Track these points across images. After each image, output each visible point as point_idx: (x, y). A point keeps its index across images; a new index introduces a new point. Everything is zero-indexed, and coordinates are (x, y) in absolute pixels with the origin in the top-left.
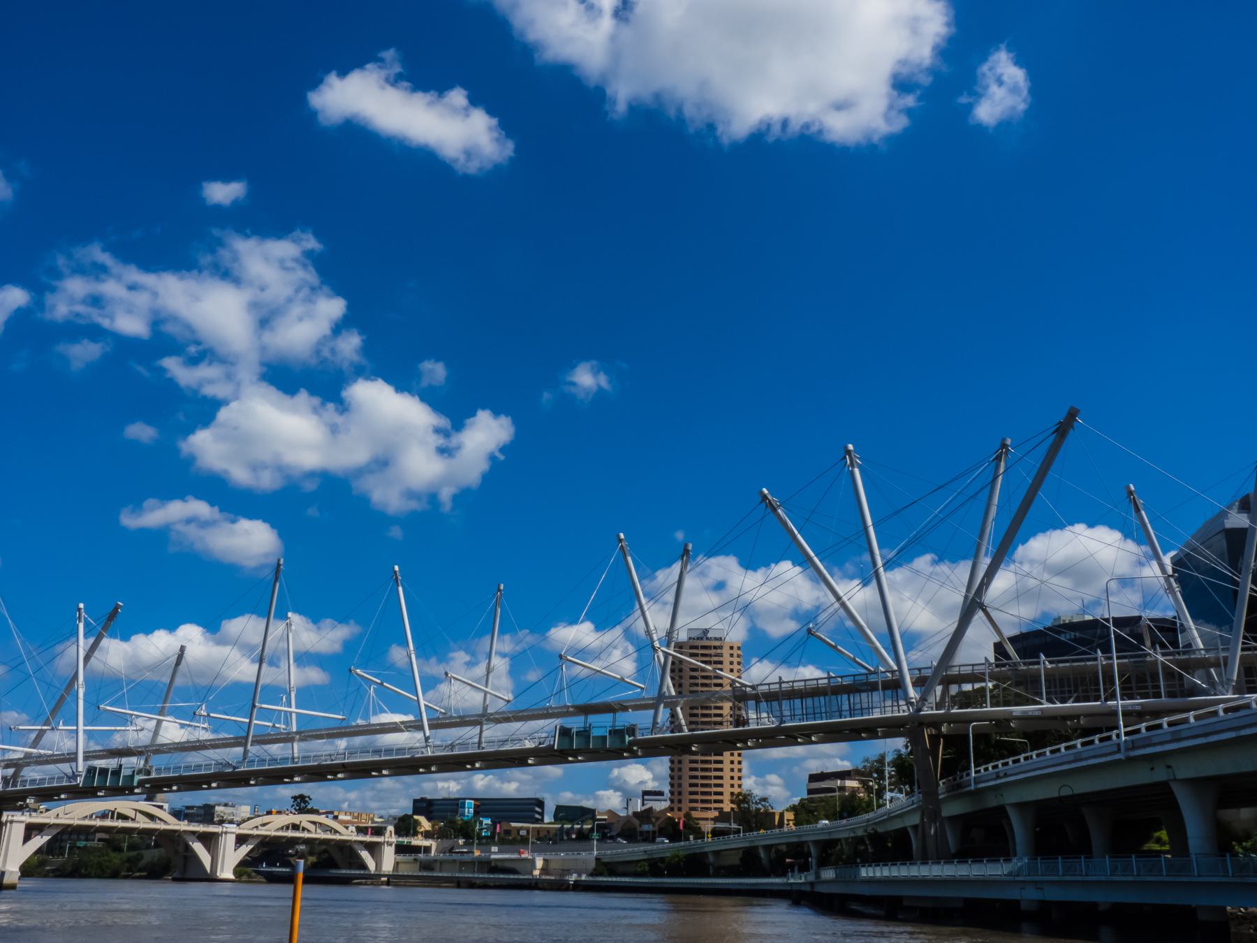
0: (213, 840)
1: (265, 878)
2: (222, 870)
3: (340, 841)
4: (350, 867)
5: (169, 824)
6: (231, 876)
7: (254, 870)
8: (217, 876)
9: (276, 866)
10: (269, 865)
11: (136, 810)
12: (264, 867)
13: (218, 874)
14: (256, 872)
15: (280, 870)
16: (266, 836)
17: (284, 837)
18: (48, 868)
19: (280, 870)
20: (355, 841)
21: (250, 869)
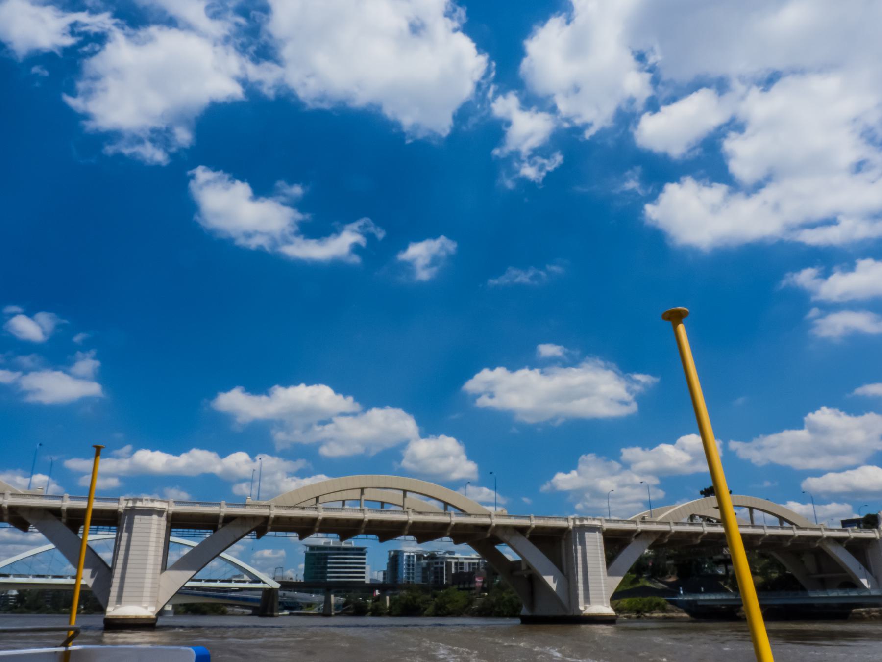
0: (563, 543)
1: (686, 611)
2: (587, 599)
3: (800, 537)
4: (823, 584)
5: (470, 515)
6: (607, 610)
7: (668, 600)
8: (581, 611)
9: (700, 592)
10: (687, 592)
11: (405, 492)
12: (683, 596)
13: (581, 608)
14: (673, 602)
15: (707, 597)
16: (664, 534)
17: (697, 534)
18: (473, 607)
19: (707, 597)
20: (829, 539)
21: (662, 600)
